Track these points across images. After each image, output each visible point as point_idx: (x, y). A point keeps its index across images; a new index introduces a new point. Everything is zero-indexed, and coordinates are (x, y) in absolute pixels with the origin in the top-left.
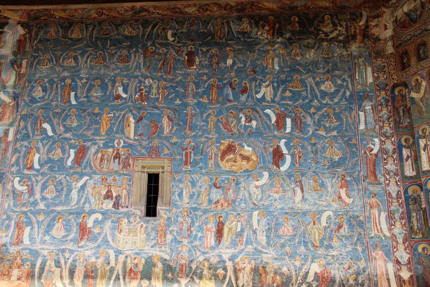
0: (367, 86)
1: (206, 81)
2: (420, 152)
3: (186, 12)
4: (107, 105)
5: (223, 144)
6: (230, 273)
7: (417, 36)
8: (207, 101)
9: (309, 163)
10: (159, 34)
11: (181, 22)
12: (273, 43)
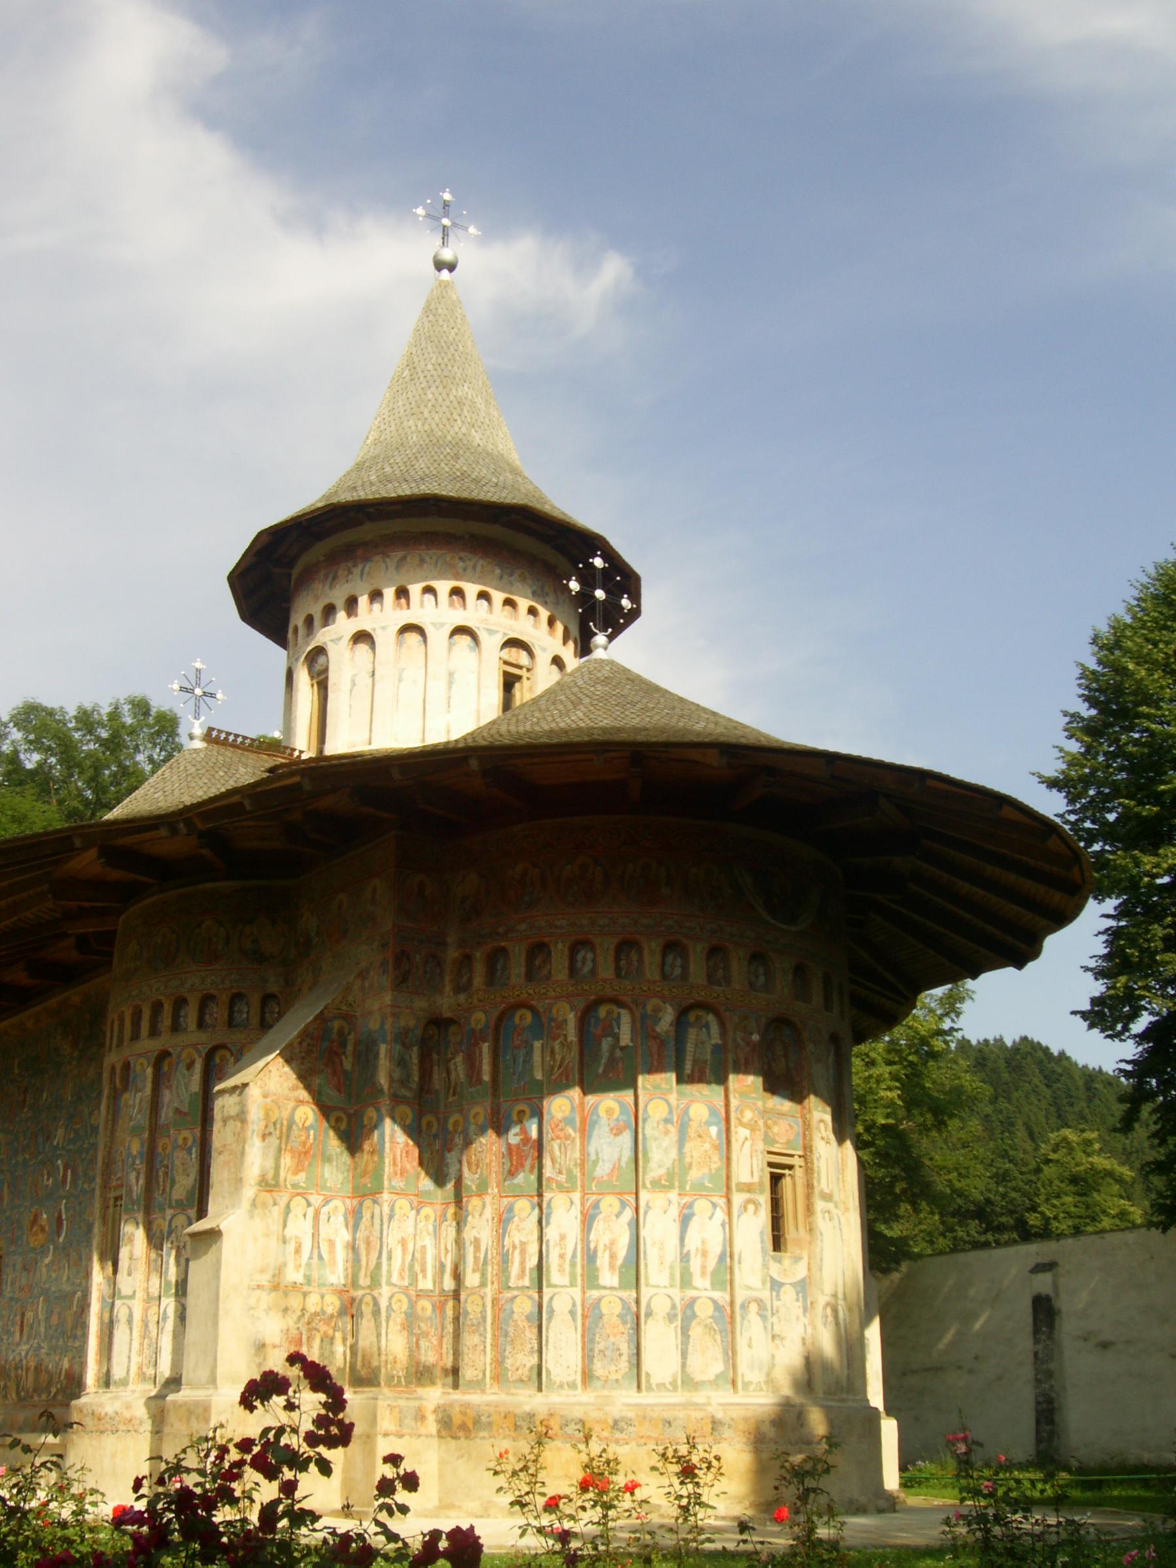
6: (24, 1374)
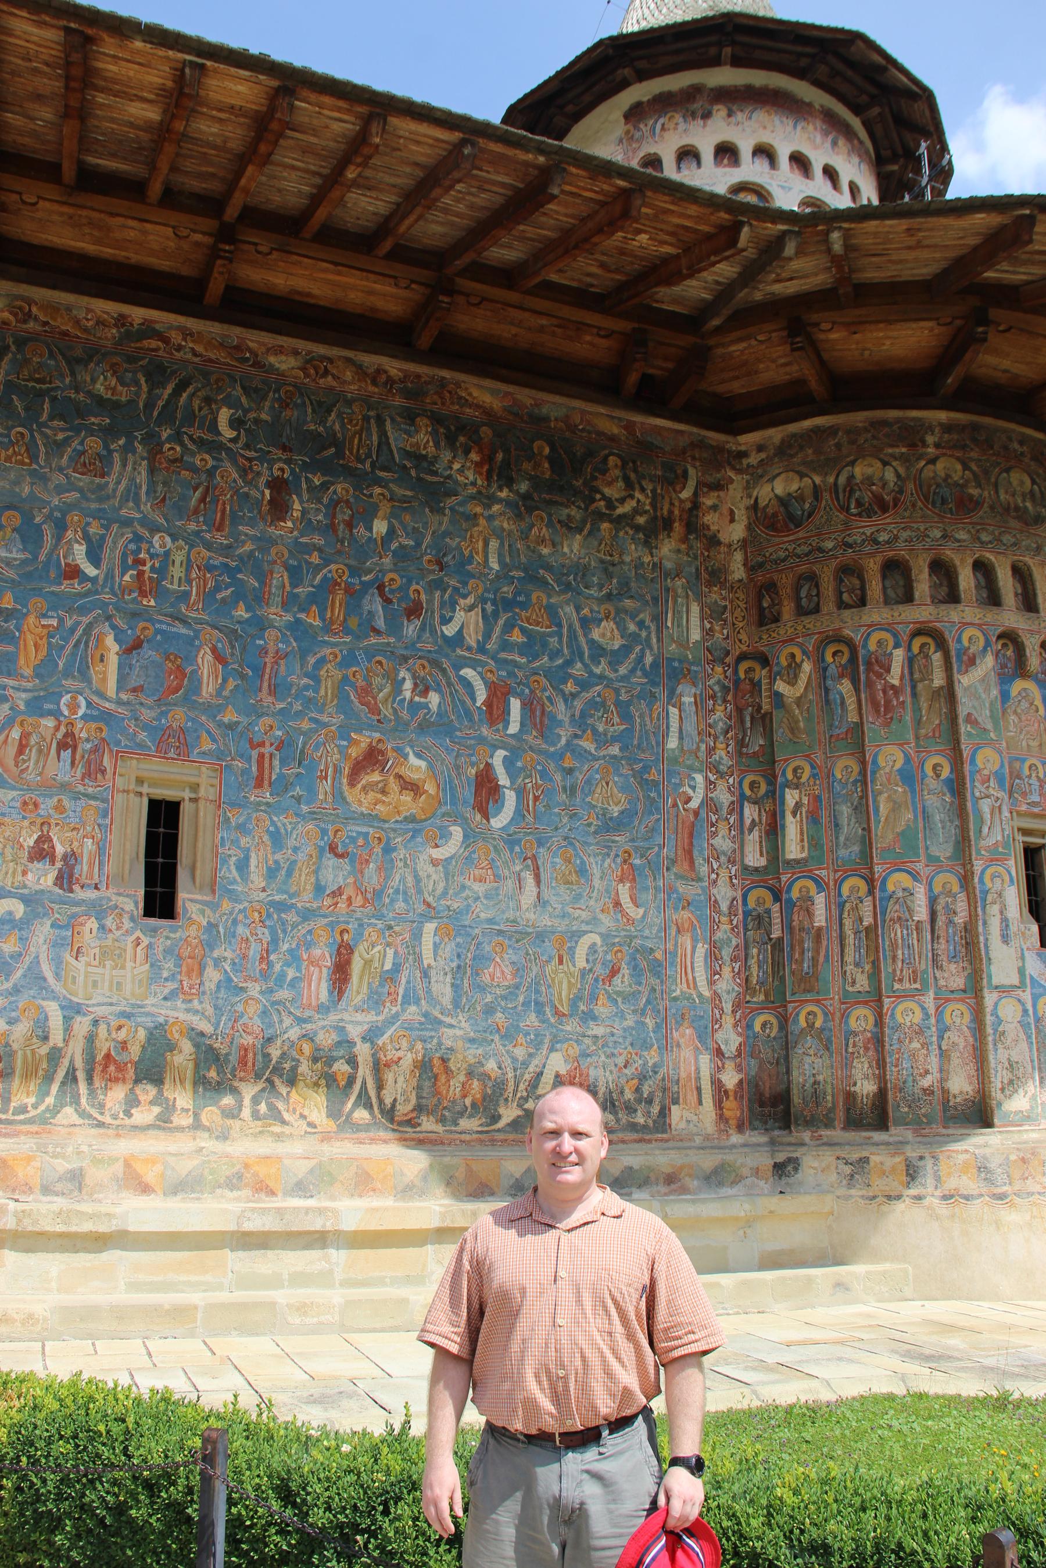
0: (688, 648)
1: (318, 569)
2: (783, 817)
3: (271, 365)
4: (38, 591)
5: (356, 742)
6: (364, 1071)
7: (799, 557)
8: (317, 623)
9: (555, 814)
10: (193, 411)
11: (256, 390)
12: (488, 498)
